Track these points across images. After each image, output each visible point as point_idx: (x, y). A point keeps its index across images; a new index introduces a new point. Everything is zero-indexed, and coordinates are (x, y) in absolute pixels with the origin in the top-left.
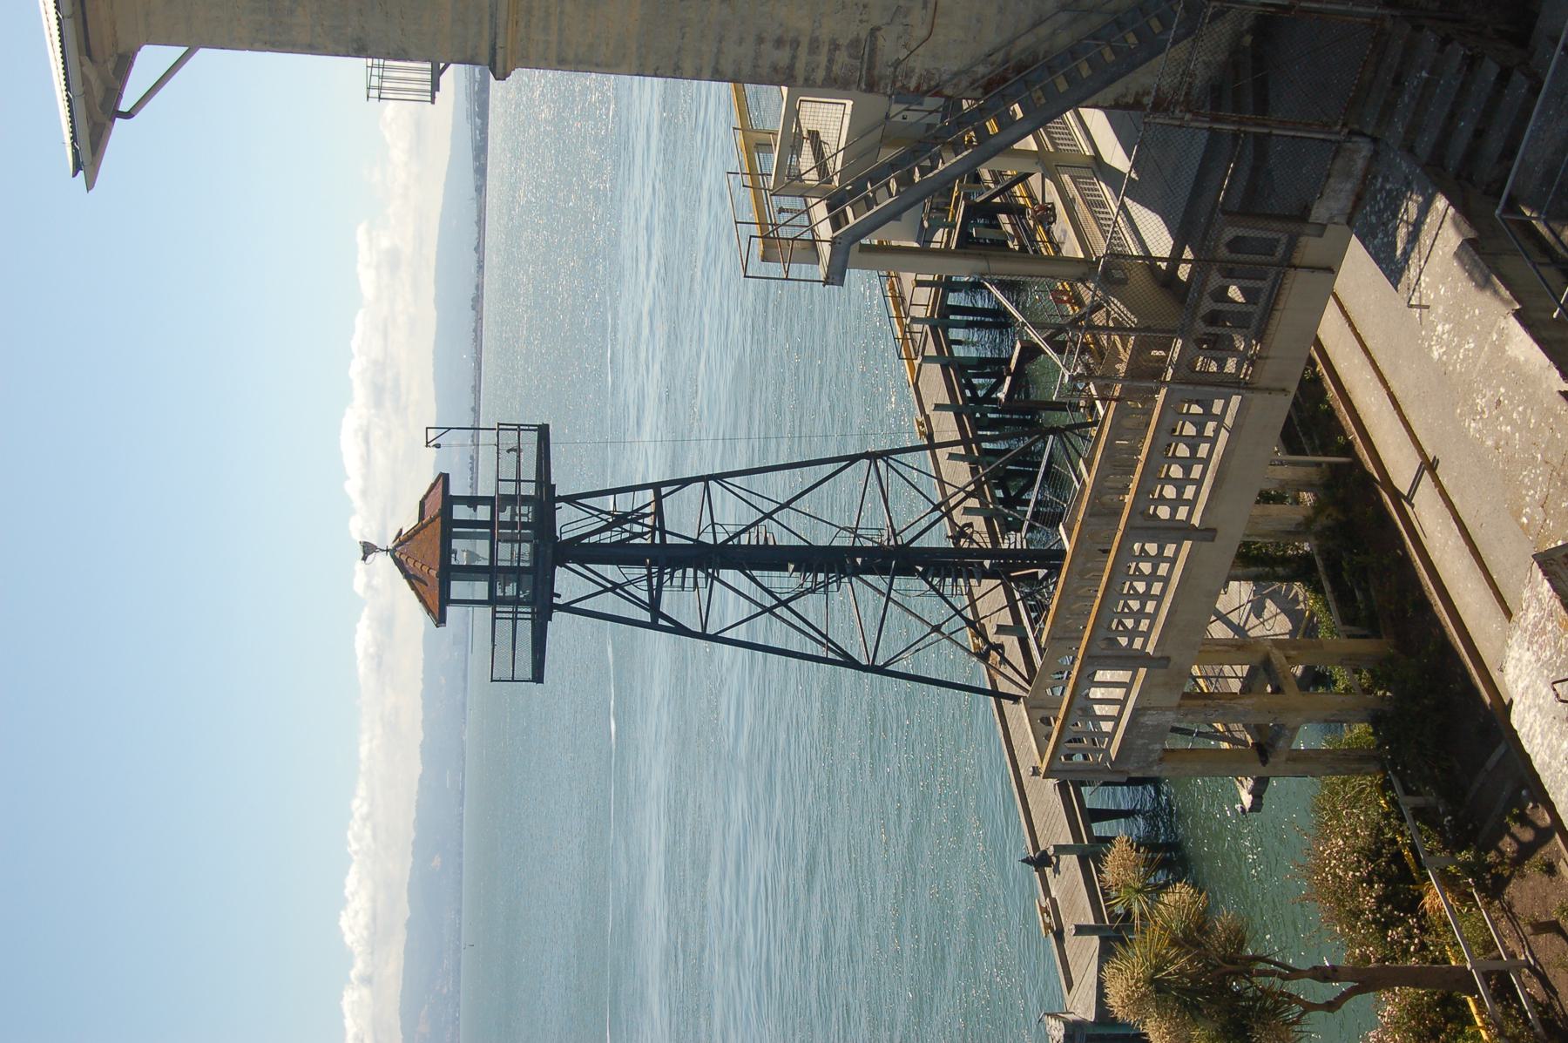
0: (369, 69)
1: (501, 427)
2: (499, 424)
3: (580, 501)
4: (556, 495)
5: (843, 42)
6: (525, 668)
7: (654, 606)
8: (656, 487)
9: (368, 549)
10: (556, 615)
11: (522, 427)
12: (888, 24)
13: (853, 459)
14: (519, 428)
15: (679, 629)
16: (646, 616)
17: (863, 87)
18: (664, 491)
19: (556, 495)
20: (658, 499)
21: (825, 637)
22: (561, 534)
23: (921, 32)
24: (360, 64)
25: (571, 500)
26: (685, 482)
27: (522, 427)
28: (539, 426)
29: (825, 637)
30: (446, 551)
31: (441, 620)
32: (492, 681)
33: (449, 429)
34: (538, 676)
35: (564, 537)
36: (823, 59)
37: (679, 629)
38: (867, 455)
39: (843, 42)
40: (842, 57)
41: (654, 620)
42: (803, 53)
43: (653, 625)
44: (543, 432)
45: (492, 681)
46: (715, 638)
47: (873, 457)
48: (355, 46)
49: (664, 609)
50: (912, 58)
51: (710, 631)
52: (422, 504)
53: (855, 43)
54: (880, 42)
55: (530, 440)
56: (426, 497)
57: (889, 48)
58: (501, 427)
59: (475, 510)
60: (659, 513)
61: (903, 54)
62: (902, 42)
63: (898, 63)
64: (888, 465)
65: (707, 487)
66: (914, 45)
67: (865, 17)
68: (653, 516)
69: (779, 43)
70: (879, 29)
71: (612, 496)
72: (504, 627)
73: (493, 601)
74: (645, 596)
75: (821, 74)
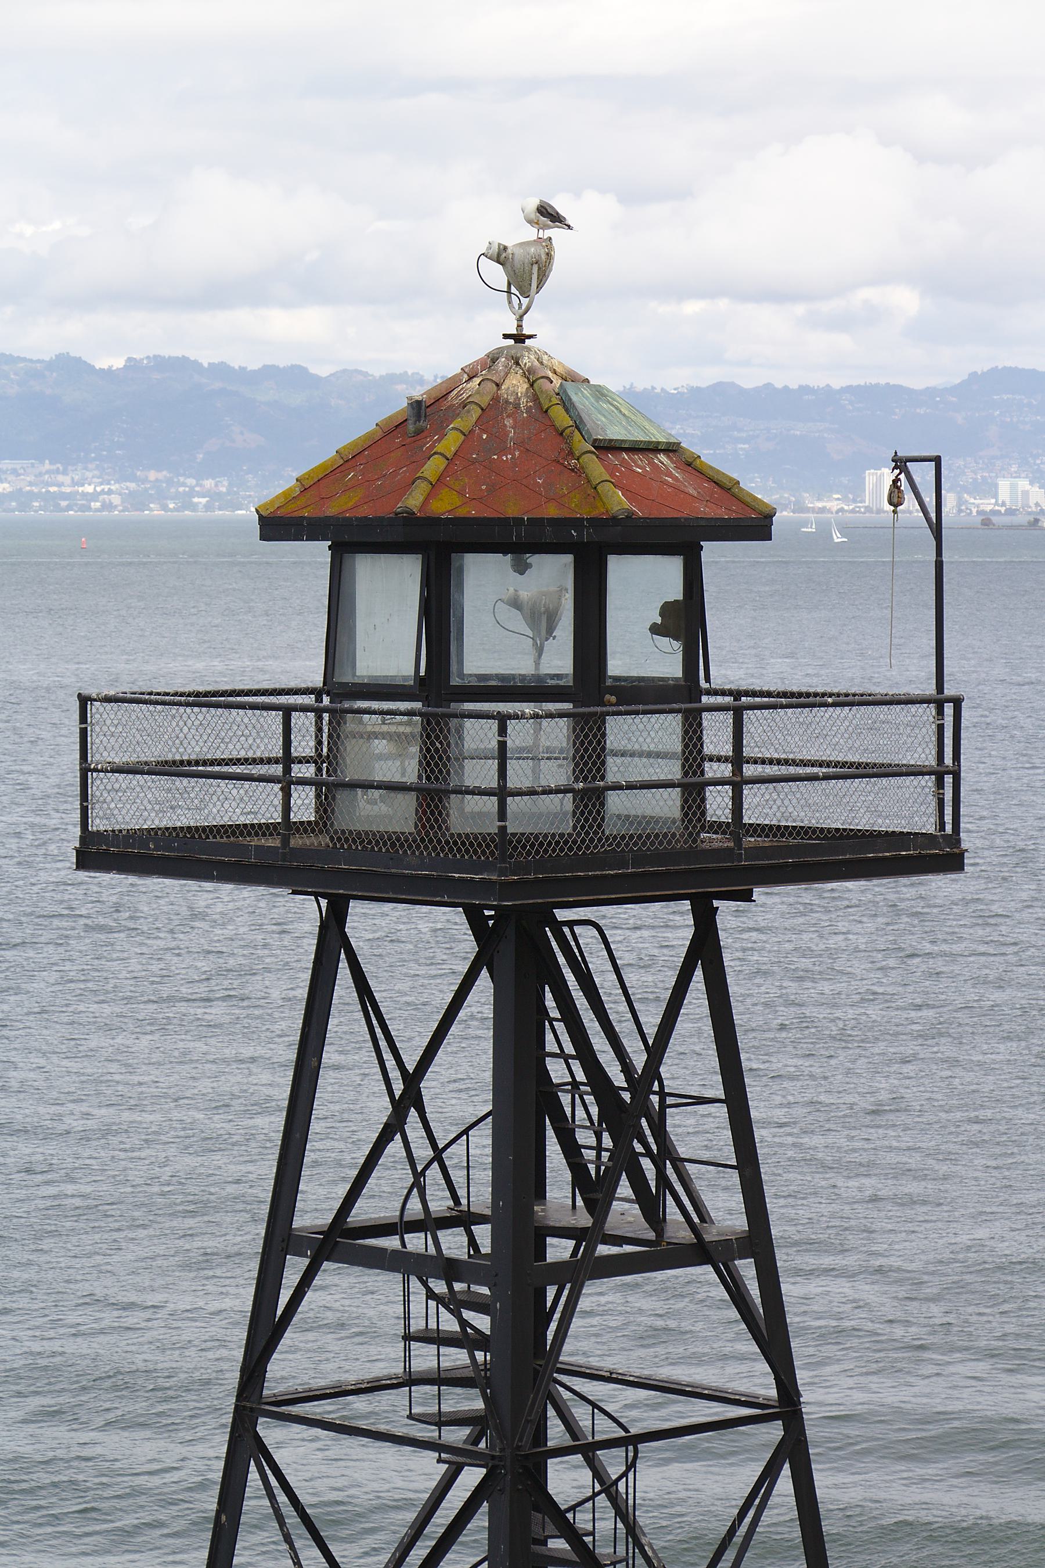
1: (949, 709)
2: (957, 702)
3: (699, 974)
4: (716, 903)
11: (948, 779)
18: (747, 1269)
19: (716, 903)
22: (571, 924)
27: (948, 779)
28: (955, 838)
32: (84, 701)
49: (331, 1273)
51: (270, 1432)
52: (672, 449)
58: (949, 709)
59: (655, 630)
68: (651, 1235)
71: (720, 1094)
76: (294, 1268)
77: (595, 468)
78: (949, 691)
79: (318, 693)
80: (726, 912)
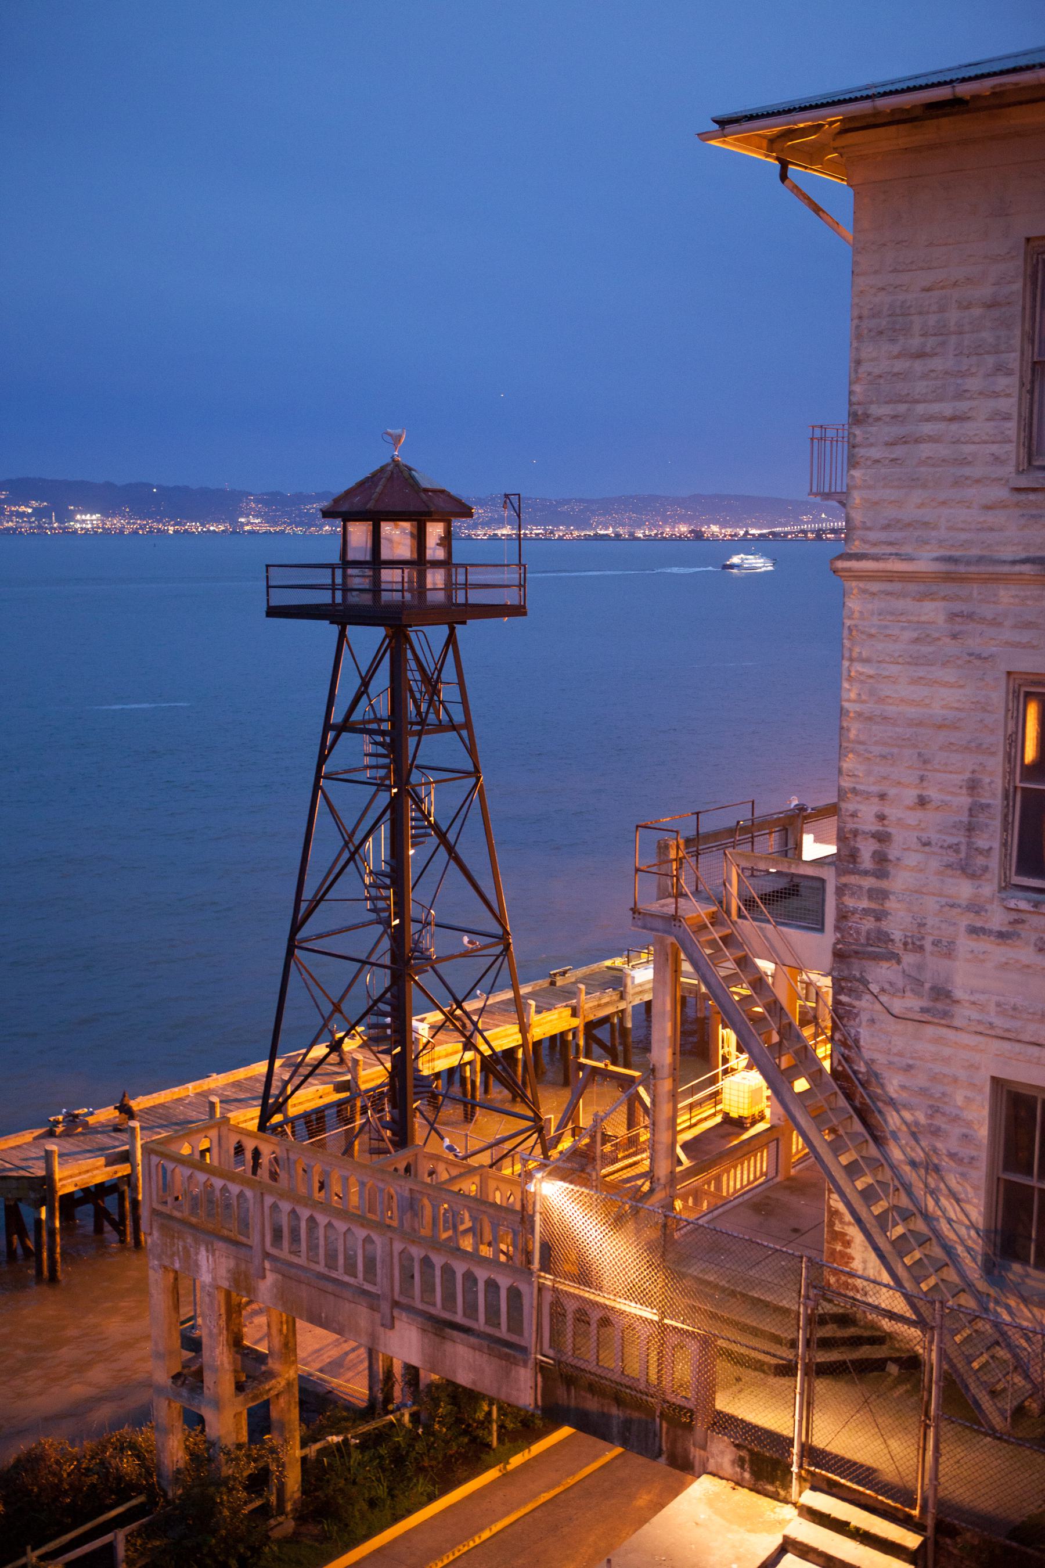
5: (884, 925)
6: (281, 598)
7: (346, 726)
8: (468, 725)
10: (335, 629)
12: (904, 972)
13: (500, 920)
14: (522, 586)
16: (337, 716)
17: (839, 946)
23: (897, 1005)
25: (451, 640)
26: (472, 751)
30: (395, 517)
32: (267, 566)
33: (519, 516)
34: (273, 612)
35: (413, 636)
36: (865, 904)
39: (884, 925)
40: (868, 924)
42: (868, 882)
43: (327, 726)
44: (518, 610)
45: (267, 566)
46: (317, 787)
47: (503, 938)
48: (860, 413)
50: (868, 997)
52: (443, 492)
53: (883, 937)
54: (885, 965)
55: (510, 597)
56: (449, 495)
57: (881, 973)
60: (440, 728)
61: (874, 988)
62: (887, 986)
63: (865, 983)
64: (498, 957)
65: (468, 774)
66: (884, 998)
67: (910, 946)
69: (881, 858)
70: (899, 962)
72: (324, 577)
73: (346, 563)
75: (850, 902)
76: (330, 736)
77: (423, 495)
78: (523, 562)
79: (332, 567)
80: (459, 628)
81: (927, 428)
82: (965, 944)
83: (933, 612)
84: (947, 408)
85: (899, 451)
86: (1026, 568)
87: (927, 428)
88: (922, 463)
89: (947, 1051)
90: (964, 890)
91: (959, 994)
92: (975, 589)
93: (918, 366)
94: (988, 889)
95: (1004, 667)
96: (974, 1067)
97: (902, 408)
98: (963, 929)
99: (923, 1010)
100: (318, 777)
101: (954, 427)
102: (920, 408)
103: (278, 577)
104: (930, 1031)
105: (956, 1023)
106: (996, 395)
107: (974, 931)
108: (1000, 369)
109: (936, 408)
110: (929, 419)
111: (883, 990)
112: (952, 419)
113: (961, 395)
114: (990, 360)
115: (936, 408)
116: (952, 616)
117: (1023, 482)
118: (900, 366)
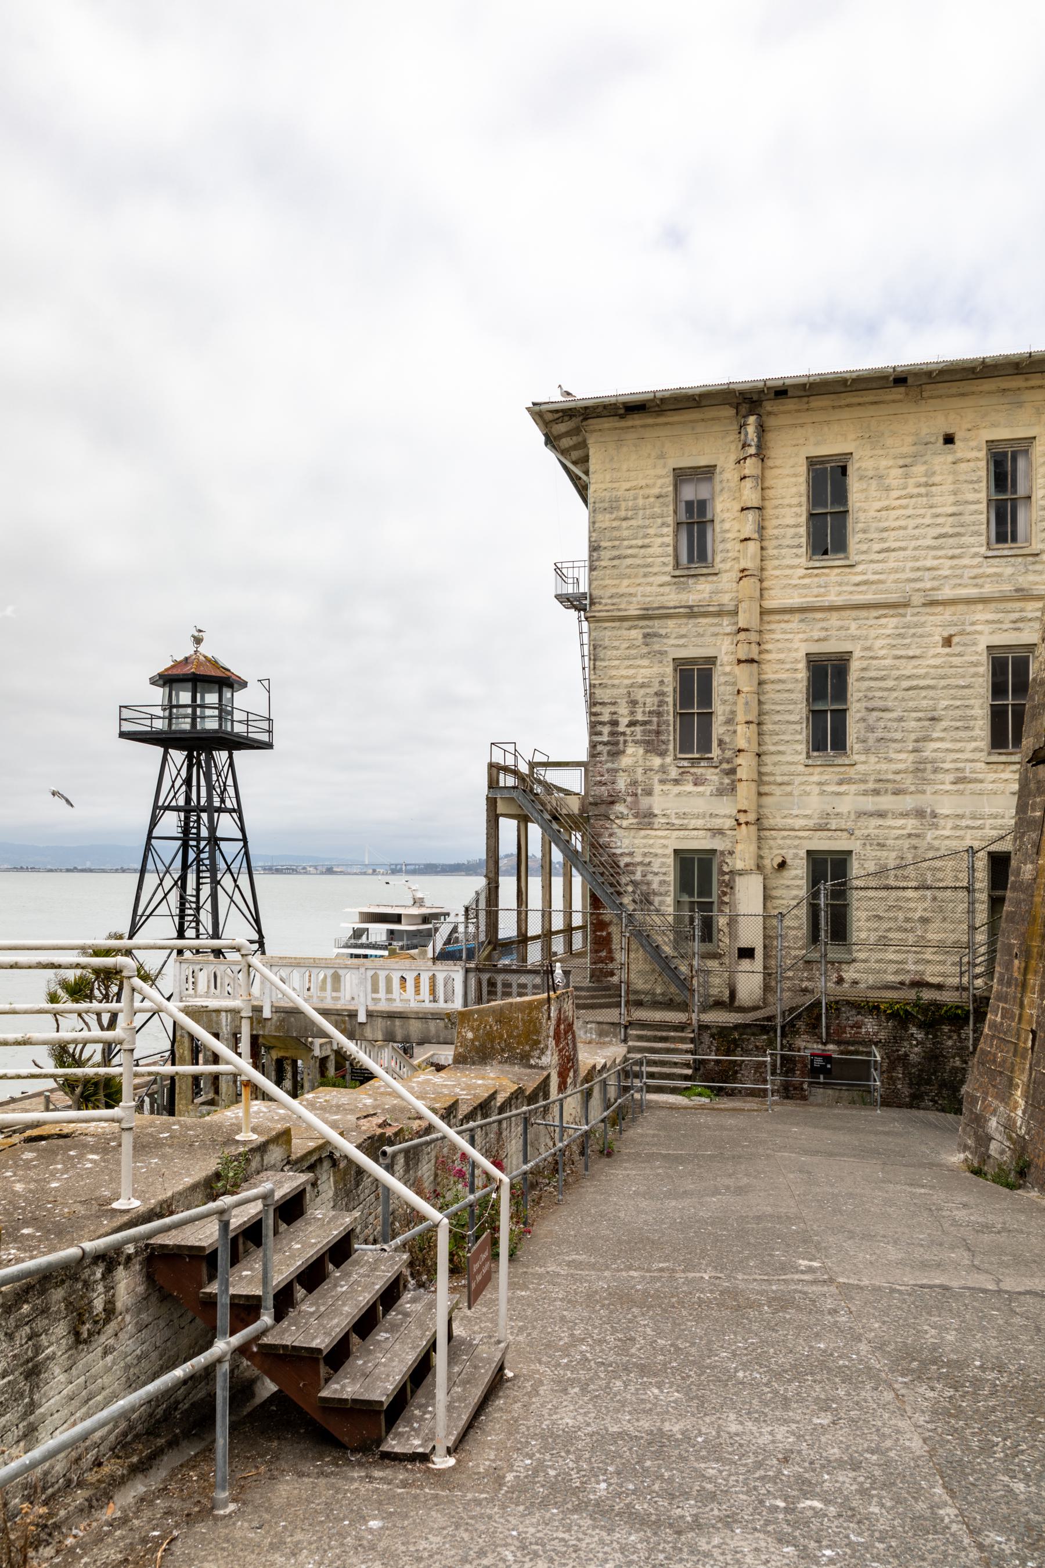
0: (571, 564)
6: (127, 727)
7: (168, 808)
9: (198, 641)
15: (154, 823)
20: (230, 811)
21: (151, 914)
24: (583, 553)
29: (151, 914)
31: (153, 682)
34: (123, 735)
37: (154, 823)
38: (261, 936)
41: (161, 808)
43: (156, 807)
44: (268, 746)
55: (264, 737)
74: (174, 803)
81: (630, 551)
82: (657, 788)
83: (636, 634)
84: (640, 542)
85: (616, 562)
86: (681, 610)
87: (630, 551)
88: (628, 567)
89: (651, 842)
90: (657, 761)
91: (656, 812)
92: (656, 622)
93: (625, 524)
94: (669, 759)
95: (672, 656)
96: (665, 846)
97: (617, 543)
98: (656, 781)
99: (638, 824)
100: (150, 837)
101: (642, 551)
102: (626, 543)
103: (126, 714)
104: (643, 833)
105: (656, 826)
106: (662, 536)
107: (662, 782)
108: (663, 524)
109: (634, 542)
110: (631, 547)
111: (617, 817)
112: (642, 547)
113: (646, 536)
114: (659, 521)
115: (634, 542)
116: (646, 636)
117: (677, 573)
118: (615, 524)
